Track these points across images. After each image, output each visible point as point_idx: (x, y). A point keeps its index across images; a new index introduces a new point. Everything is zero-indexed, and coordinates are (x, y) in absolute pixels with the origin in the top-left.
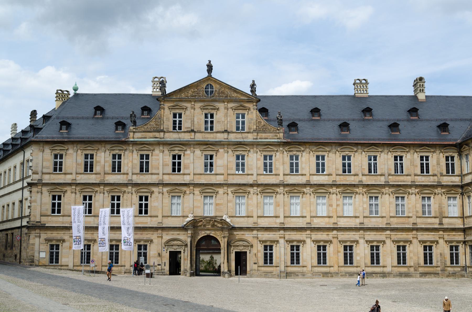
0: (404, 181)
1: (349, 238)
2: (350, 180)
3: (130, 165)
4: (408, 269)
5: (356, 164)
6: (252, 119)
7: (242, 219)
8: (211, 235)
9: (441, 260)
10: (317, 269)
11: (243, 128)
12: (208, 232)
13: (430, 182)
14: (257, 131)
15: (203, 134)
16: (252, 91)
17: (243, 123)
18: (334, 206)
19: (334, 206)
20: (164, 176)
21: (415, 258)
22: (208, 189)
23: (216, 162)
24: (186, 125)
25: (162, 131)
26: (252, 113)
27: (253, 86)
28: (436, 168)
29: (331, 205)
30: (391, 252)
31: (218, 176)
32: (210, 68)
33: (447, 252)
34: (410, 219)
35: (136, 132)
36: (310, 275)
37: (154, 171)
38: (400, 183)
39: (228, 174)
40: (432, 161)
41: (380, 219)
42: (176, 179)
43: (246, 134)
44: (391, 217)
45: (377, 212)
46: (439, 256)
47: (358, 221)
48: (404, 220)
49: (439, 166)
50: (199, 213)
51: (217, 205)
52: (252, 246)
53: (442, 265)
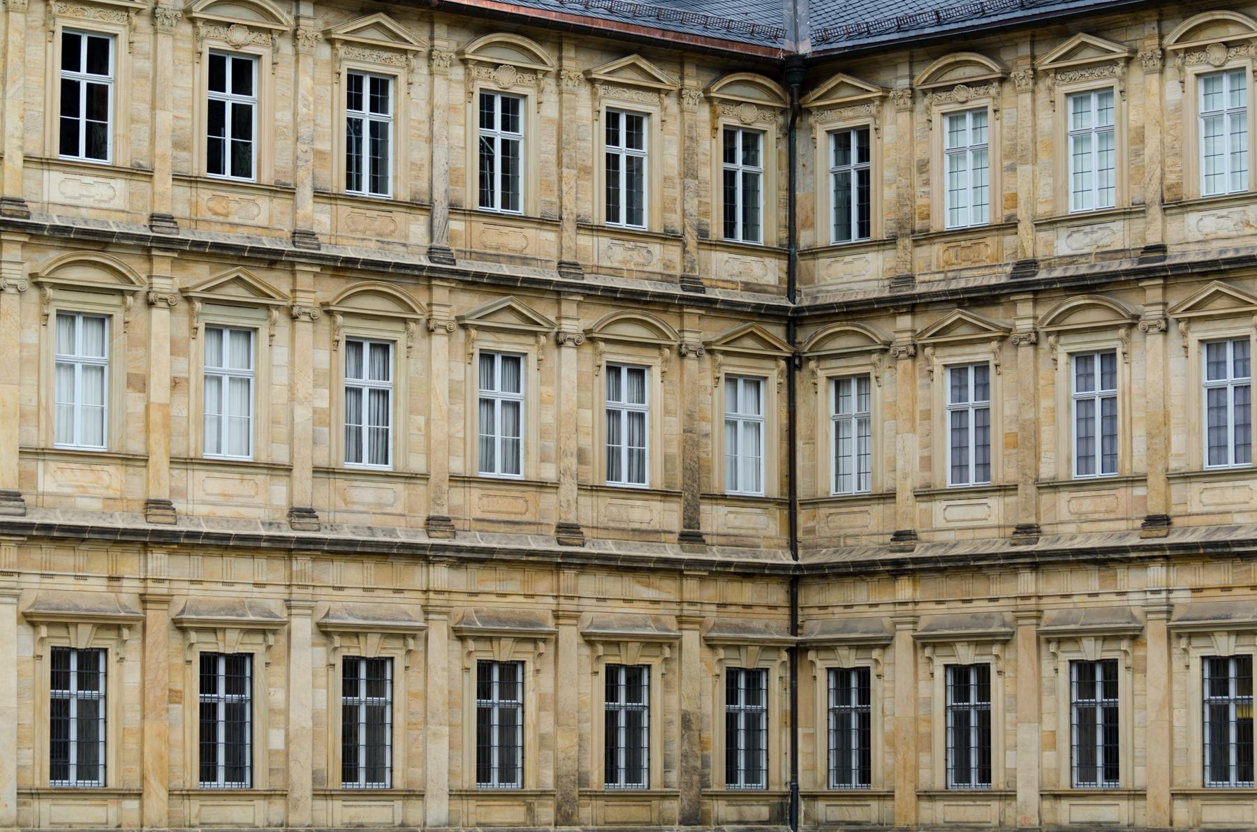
0: (525, 260)
1: (231, 609)
2: (250, 217)
4: (530, 810)
9: (685, 756)
13: (650, 276)
18: (159, 390)
21: (566, 742)
28: (677, 193)
29: (139, 383)
30: (453, 704)
33: (713, 707)
34: (548, 500)
38: (506, 270)
40: (661, 151)
41: (399, 487)
44: (455, 479)
46: (676, 730)
47: (278, 494)
48: (519, 505)
49: (690, 182)
53: (689, 785)
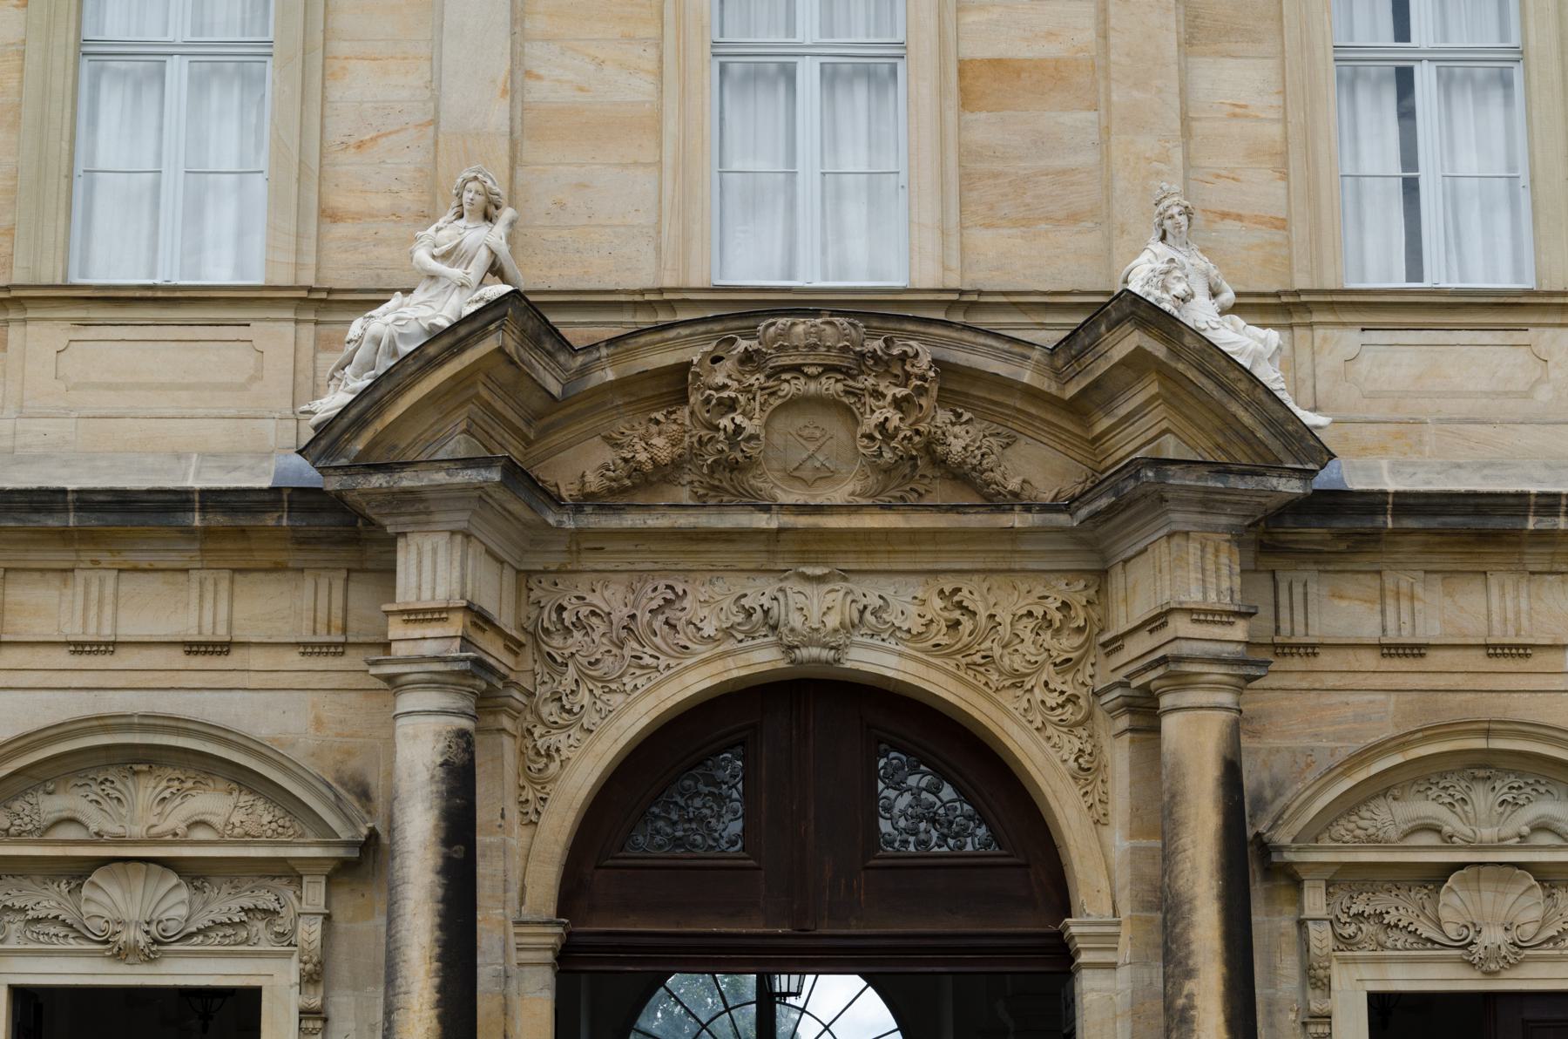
8: (873, 659)
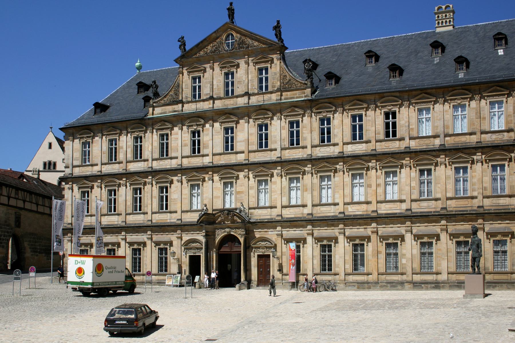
3: (150, 147)
5: (402, 122)
6: (275, 74)
7: (264, 211)
10: (351, 278)
11: (267, 87)
12: (227, 230)
14: (281, 90)
15: (223, 100)
16: (276, 35)
17: (267, 79)
19: (374, 187)
20: (183, 159)
22: (228, 172)
23: (236, 135)
24: (206, 91)
25: (182, 102)
26: (276, 64)
27: (277, 28)
29: (370, 186)
31: (239, 155)
32: (231, 12)
34: (475, 201)
35: (156, 107)
36: (342, 286)
37: (173, 155)
39: (250, 152)
42: (196, 162)
43: (269, 95)
44: (448, 199)
45: (429, 192)
48: (466, 203)
50: (218, 205)
51: (238, 193)
52: (275, 247)
